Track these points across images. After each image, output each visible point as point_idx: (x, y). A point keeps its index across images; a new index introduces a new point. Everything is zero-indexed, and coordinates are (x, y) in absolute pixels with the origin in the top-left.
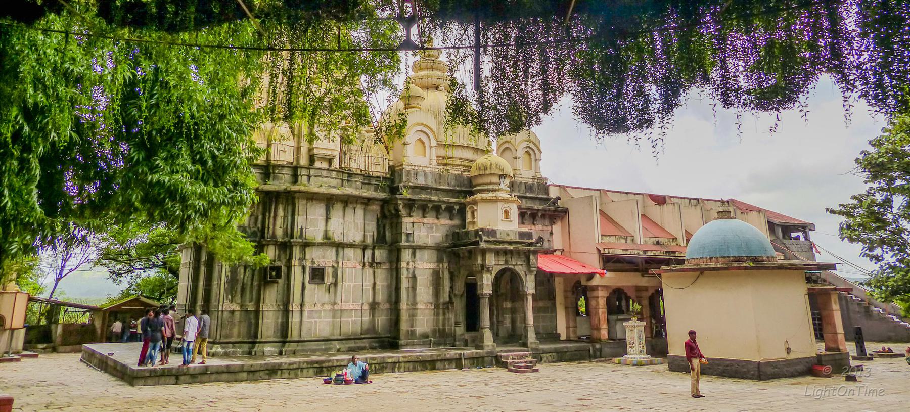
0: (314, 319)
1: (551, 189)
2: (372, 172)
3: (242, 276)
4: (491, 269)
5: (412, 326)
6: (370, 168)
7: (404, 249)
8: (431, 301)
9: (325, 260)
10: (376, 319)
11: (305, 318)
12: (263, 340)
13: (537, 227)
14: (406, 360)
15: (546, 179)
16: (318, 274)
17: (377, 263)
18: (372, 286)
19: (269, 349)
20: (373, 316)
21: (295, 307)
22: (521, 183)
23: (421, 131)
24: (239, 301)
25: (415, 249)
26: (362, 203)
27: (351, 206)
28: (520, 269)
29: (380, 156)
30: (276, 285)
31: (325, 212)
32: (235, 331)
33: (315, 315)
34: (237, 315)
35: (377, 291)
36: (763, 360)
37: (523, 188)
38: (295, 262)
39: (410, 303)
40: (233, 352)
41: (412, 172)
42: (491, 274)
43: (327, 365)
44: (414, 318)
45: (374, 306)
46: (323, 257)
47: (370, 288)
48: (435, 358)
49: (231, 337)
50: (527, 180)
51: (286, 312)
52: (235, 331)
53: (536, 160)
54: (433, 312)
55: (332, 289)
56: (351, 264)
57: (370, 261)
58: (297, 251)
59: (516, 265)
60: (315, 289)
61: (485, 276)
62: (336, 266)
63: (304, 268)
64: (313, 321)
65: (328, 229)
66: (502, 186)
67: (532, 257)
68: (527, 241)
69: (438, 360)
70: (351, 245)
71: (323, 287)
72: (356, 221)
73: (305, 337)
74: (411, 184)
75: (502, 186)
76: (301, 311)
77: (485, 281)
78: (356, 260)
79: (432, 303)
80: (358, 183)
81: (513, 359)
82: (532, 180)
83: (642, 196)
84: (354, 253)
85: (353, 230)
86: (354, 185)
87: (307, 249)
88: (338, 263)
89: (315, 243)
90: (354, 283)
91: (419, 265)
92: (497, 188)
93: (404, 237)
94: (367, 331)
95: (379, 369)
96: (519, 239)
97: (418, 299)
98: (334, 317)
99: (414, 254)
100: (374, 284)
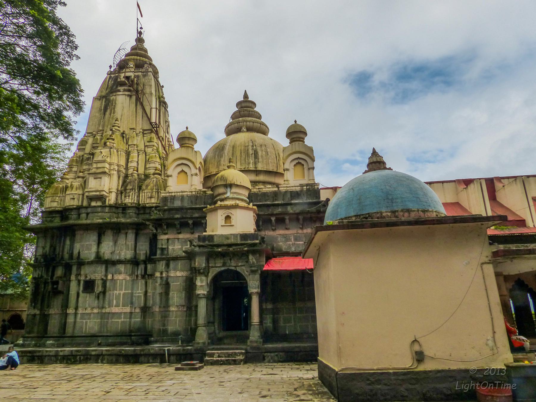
0: (85, 319)
1: (321, 190)
2: (148, 203)
3: (42, 290)
4: (202, 271)
5: (164, 325)
6: (145, 201)
7: (159, 261)
8: (184, 304)
9: (96, 275)
10: (147, 320)
11: (78, 320)
12: (49, 335)
13: (305, 231)
14: (109, 353)
15: (318, 184)
16: (89, 286)
17: (148, 275)
18: (144, 293)
19: (51, 342)
20: (144, 318)
21: (71, 311)
22: (286, 192)
23: (182, 164)
24: (40, 308)
25: (169, 260)
26: (133, 229)
27: (123, 231)
28: (244, 270)
29: (154, 190)
30: (62, 295)
31: (97, 238)
32: (36, 330)
33: (86, 317)
34: (38, 317)
35: (148, 298)
36: (342, 370)
37: (289, 195)
38: (73, 277)
39: (162, 306)
40: (28, 344)
41: (169, 198)
42: (207, 276)
43: (38, 354)
44: (166, 319)
45: (145, 310)
46: (95, 272)
47: (142, 295)
48: (139, 353)
49: (33, 332)
50: (294, 188)
51: (66, 315)
52: (36, 330)
53: (309, 169)
54: (185, 313)
55: (101, 297)
56: (121, 277)
57: (143, 273)
58: (74, 268)
59: (239, 266)
60: (87, 297)
61: (198, 278)
62: (105, 278)
63: (79, 281)
64: (84, 321)
65: (99, 251)
66: (228, 194)
67: (251, 257)
68: (249, 242)
69: (141, 355)
70: (120, 262)
71: (93, 296)
72: (127, 243)
73: (77, 333)
74: (166, 208)
75: (228, 194)
76: (76, 314)
77: (198, 283)
78: (126, 273)
79: (183, 306)
80: (131, 214)
81: (219, 357)
82: (300, 188)
83: (454, 183)
84: (125, 268)
85: (124, 250)
86: (128, 216)
87: (82, 267)
88: (106, 276)
89: (85, 262)
90: (123, 291)
91: (172, 274)
92: (223, 197)
93: (159, 252)
94: (139, 330)
95: (83, 360)
96: (241, 240)
97: (171, 302)
98: (101, 319)
99: (168, 265)
100: (146, 293)
